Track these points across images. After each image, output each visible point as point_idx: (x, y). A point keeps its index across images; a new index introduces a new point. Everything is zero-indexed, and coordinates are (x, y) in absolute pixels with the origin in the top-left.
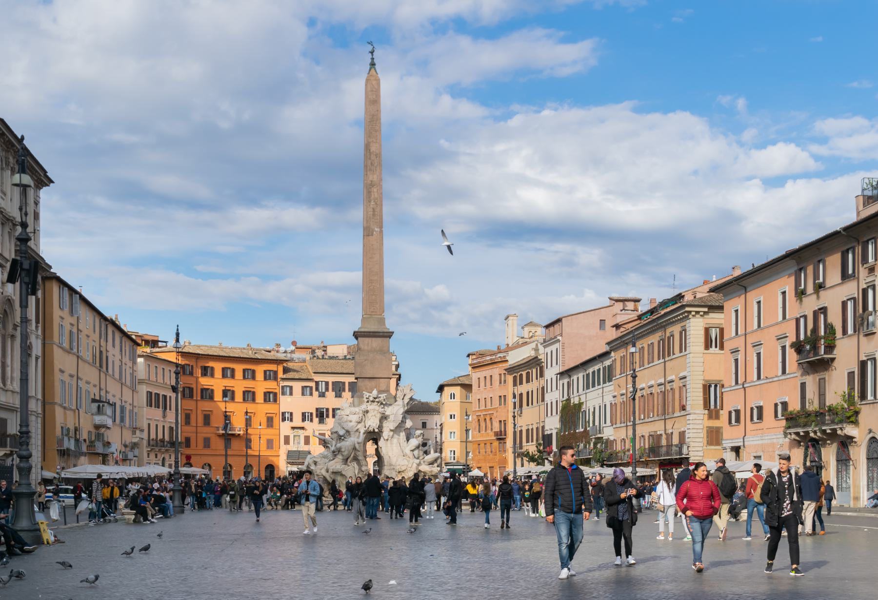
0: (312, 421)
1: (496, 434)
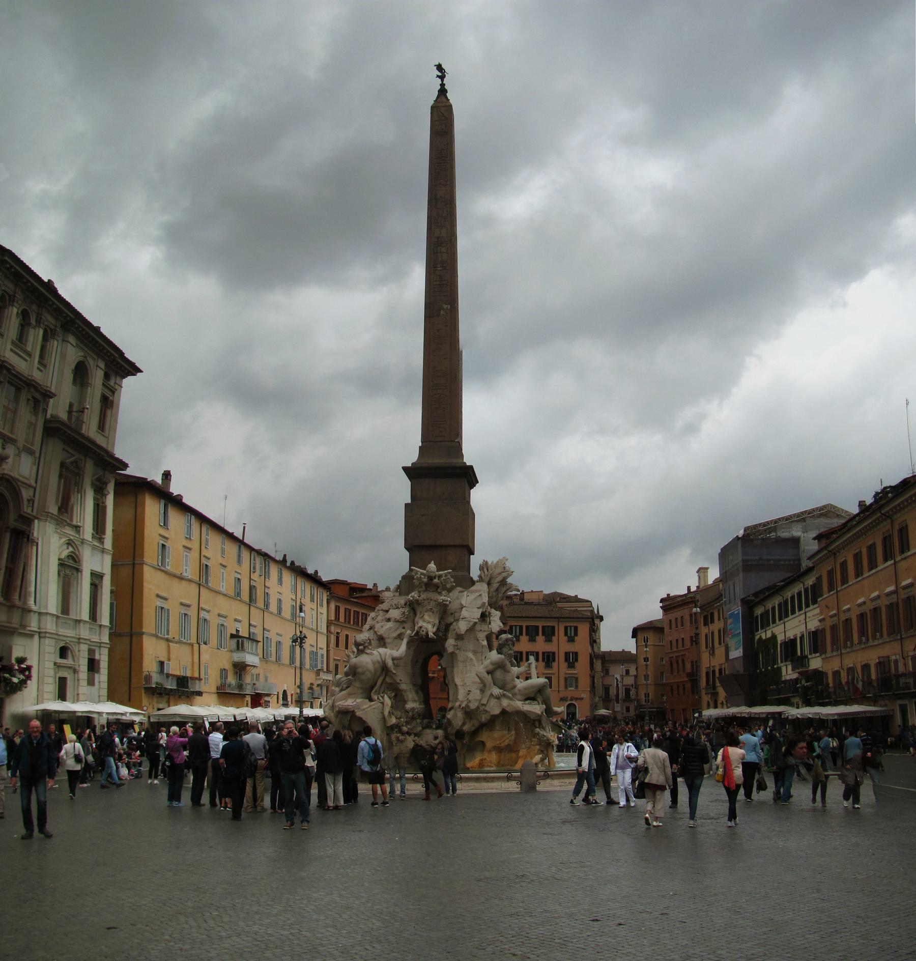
1: (689, 675)
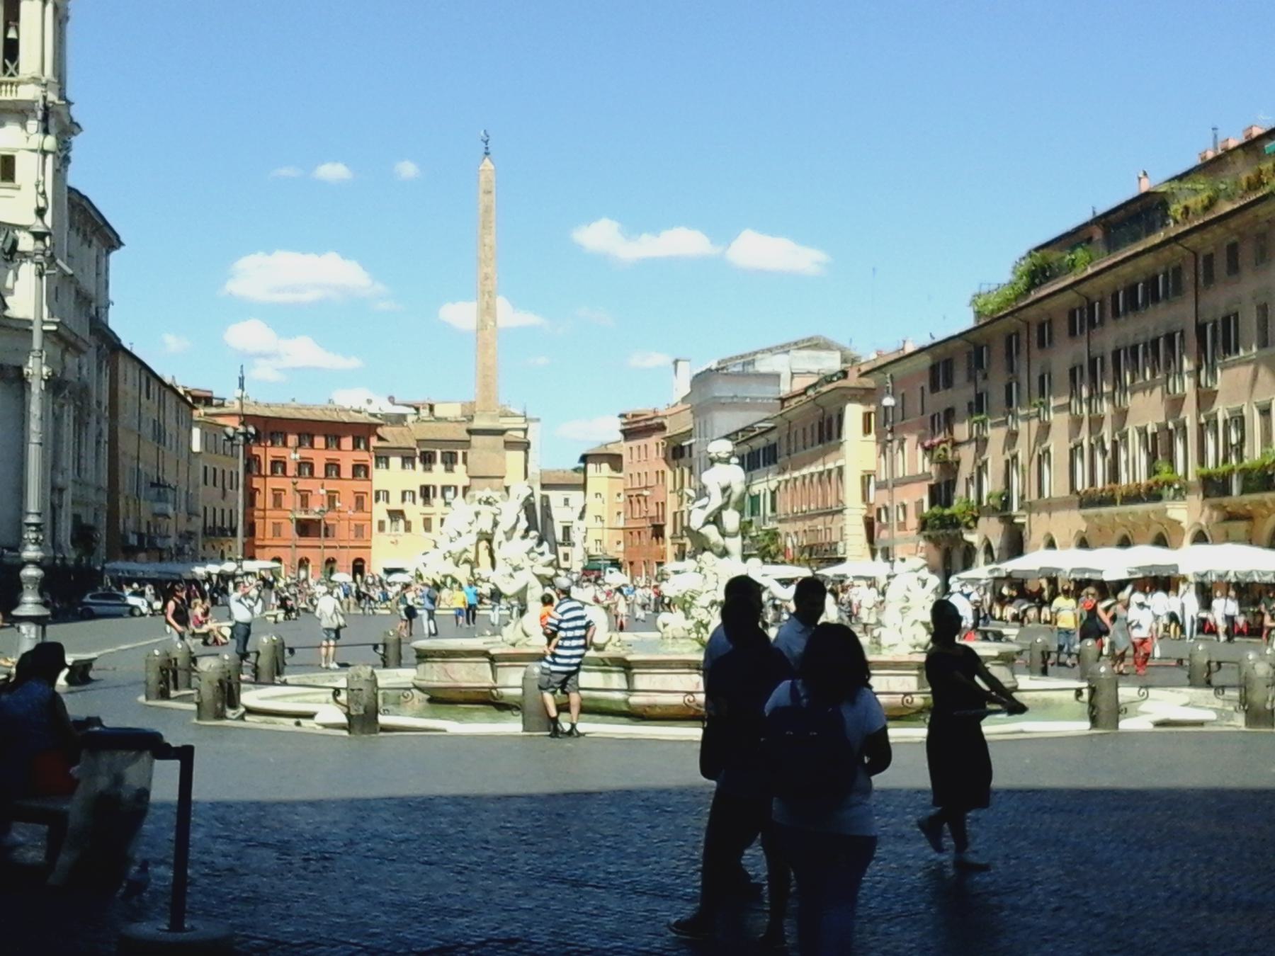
0: (414, 501)
